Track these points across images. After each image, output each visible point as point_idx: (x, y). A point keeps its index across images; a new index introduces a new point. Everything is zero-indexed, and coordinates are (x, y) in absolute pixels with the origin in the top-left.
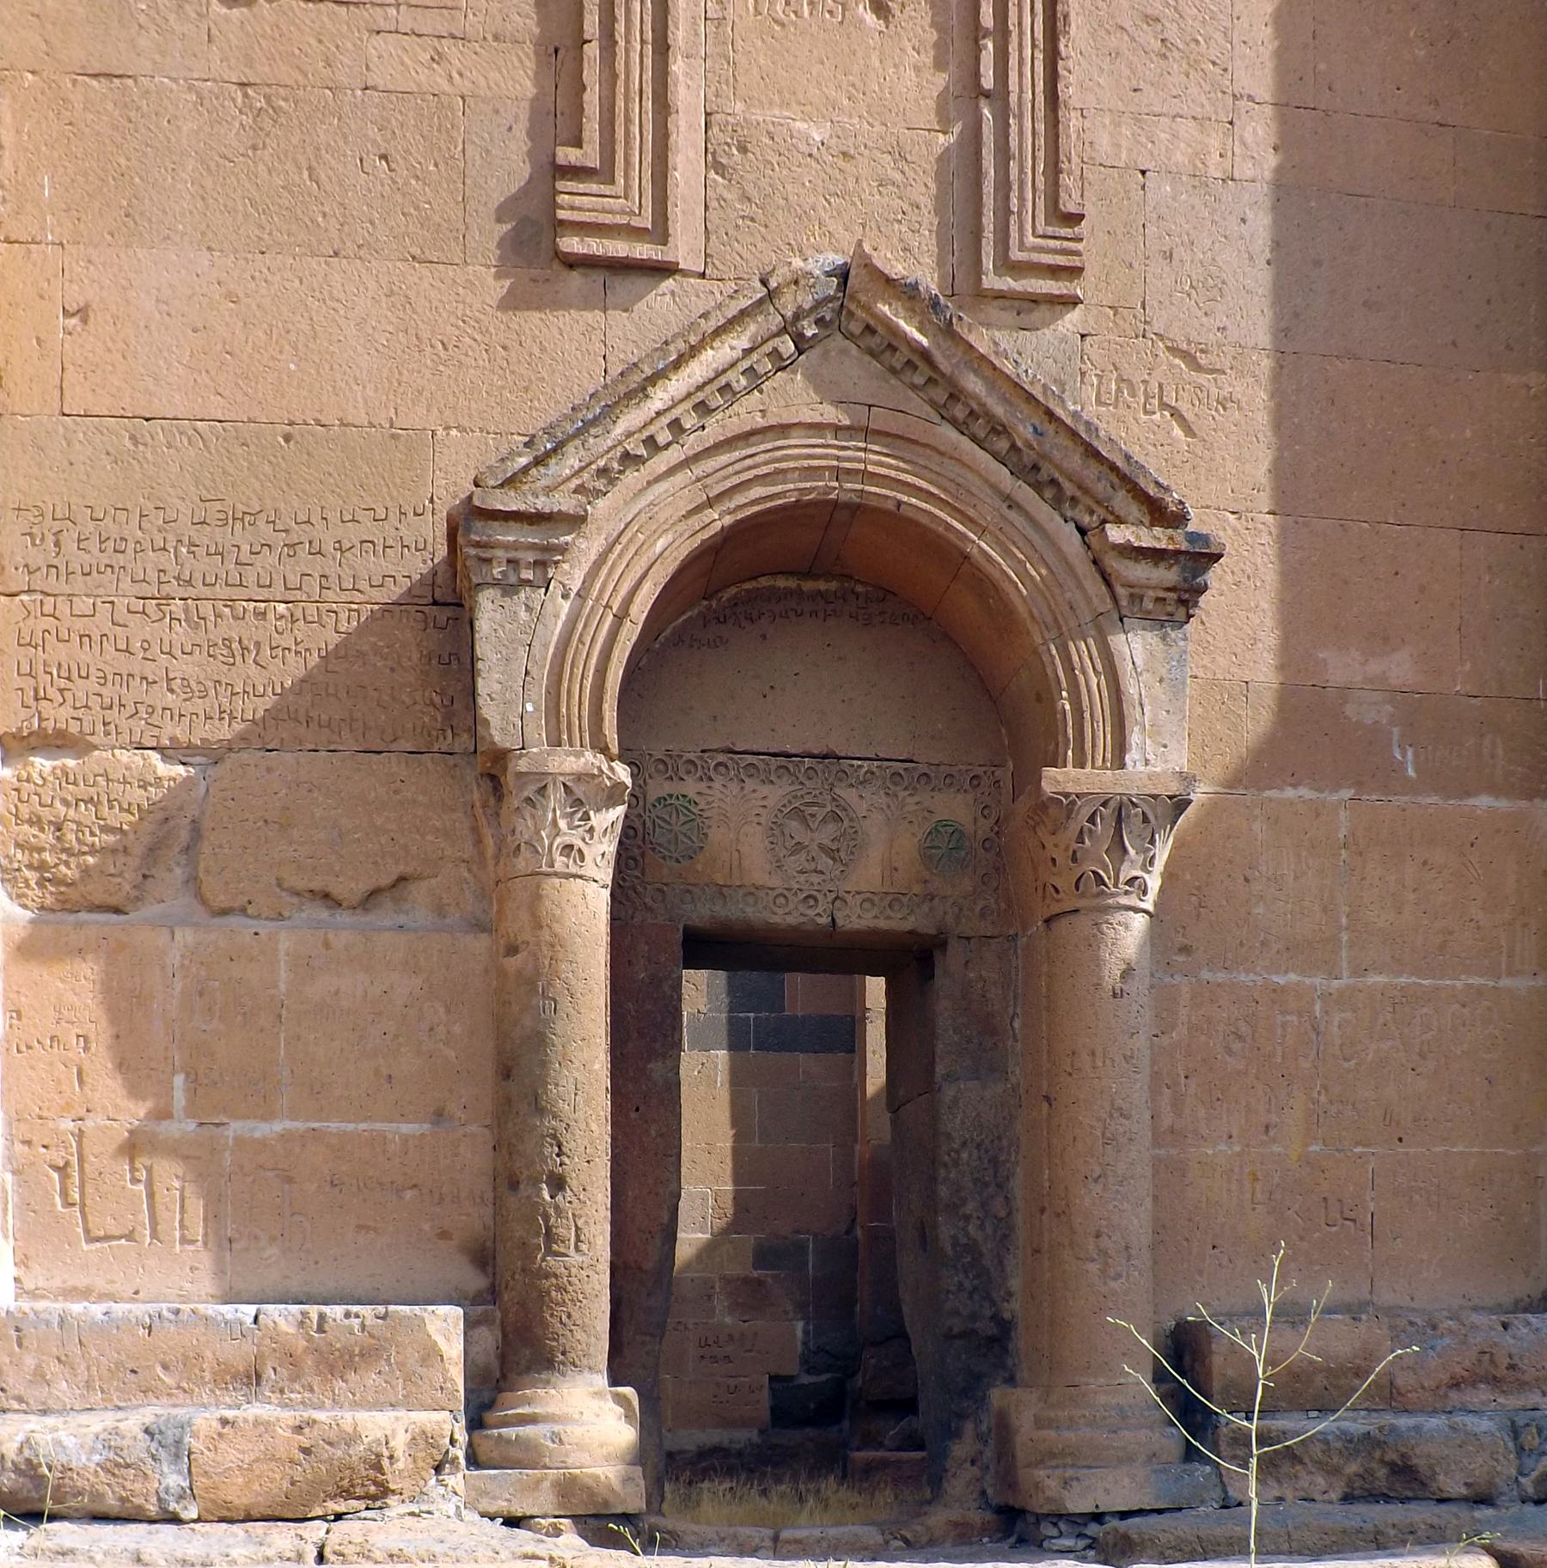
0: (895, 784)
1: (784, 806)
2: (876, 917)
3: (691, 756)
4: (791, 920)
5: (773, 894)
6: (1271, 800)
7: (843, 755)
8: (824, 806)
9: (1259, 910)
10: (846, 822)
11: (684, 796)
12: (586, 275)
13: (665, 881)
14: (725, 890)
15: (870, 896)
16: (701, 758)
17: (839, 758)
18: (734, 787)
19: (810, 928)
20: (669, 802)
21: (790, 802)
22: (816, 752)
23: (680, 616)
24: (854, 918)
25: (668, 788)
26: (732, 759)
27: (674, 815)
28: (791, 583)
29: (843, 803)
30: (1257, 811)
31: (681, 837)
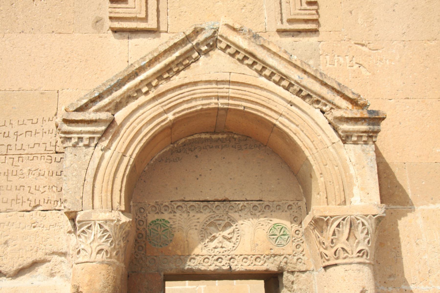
0: (256, 210)
1: (207, 221)
2: (249, 265)
3: (167, 204)
4: (212, 268)
6: (423, 210)
7: (231, 199)
8: (224, 220)
9: (426, 257)
11: (164, 220)
12: (121, 35)
13: (155, 254)
14: (182, 257)
15: (246, 256)
16: (171, 204)
17: (230, 201)
18: (185, 215)
19: (221, 271)
20: (157, 222)
21: (209, 220)
22: (220, 199)
23: (161, 151)
26: (184, 204)
27: (159, 228)
28: (208, 136)
31: (162, 236)
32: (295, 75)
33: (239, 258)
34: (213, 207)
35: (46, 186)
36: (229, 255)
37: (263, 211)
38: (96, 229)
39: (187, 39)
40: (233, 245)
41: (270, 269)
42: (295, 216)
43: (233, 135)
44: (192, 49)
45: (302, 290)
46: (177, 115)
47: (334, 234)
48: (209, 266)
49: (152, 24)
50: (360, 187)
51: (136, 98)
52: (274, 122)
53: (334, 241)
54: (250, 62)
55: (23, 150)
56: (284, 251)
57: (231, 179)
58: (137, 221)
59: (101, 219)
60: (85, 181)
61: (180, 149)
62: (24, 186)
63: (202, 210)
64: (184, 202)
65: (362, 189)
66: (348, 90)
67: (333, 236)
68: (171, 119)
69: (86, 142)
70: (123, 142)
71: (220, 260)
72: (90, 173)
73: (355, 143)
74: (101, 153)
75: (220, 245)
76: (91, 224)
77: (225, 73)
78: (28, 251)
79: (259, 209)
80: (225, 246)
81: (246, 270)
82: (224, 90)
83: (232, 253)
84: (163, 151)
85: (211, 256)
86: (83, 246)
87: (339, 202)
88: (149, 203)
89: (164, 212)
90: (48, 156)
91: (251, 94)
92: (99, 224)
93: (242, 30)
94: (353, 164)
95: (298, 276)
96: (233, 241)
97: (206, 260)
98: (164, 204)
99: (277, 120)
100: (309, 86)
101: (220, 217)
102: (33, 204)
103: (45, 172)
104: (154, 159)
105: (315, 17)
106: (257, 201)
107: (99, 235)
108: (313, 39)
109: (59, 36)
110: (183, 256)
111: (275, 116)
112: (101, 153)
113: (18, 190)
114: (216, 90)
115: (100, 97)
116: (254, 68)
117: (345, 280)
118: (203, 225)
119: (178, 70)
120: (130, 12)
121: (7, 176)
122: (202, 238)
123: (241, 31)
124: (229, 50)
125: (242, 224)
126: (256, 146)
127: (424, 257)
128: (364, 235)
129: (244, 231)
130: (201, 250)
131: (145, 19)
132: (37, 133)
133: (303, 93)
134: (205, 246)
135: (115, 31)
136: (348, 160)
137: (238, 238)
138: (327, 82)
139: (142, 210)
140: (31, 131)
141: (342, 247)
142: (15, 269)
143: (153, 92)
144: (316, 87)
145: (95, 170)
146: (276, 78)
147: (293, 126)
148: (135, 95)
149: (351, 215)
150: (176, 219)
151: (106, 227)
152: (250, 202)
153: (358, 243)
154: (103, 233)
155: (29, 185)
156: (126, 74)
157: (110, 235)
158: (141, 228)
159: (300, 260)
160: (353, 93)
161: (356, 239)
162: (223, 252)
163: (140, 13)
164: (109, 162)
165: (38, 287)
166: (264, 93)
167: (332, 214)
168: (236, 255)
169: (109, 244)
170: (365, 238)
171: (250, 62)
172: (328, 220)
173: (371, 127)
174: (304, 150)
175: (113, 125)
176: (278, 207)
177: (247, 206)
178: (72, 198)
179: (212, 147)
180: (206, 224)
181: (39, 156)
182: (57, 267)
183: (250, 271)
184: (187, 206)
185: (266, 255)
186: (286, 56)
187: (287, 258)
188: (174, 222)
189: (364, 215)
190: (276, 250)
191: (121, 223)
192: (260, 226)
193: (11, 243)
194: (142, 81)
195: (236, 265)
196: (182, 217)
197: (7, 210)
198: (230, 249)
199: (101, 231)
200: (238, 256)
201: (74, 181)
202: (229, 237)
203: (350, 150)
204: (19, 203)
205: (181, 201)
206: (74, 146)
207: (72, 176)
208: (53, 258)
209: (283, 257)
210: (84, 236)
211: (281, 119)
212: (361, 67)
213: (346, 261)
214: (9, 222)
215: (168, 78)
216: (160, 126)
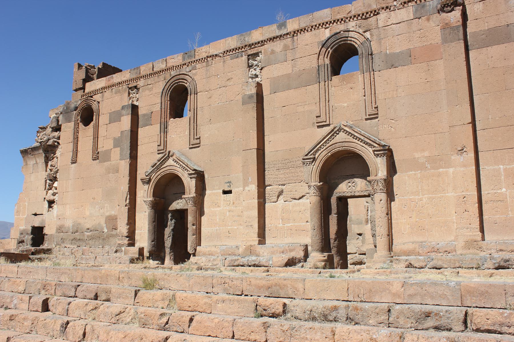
4: (349, 195)
9: (407, 189)
28: (348, 155)
32: (362, 138)
47: (373, 185)
49: (328, 123)
51: (320, 150)
69: (309, 164)
73: (380, 157)
100: (366, 141)
105: (376, 113)
108: (377, 120)
111: (358, 151)
115: (311, 151)
124: (344, 132)
128: (381, 184)
131: (326, 122)
133: (365, 143)
135: (319, 127)
144: (369, 141)
151: (315, 187)
186: (359, 132)
190: (368, 189)
213: (377, 192)
215: (328, 143)
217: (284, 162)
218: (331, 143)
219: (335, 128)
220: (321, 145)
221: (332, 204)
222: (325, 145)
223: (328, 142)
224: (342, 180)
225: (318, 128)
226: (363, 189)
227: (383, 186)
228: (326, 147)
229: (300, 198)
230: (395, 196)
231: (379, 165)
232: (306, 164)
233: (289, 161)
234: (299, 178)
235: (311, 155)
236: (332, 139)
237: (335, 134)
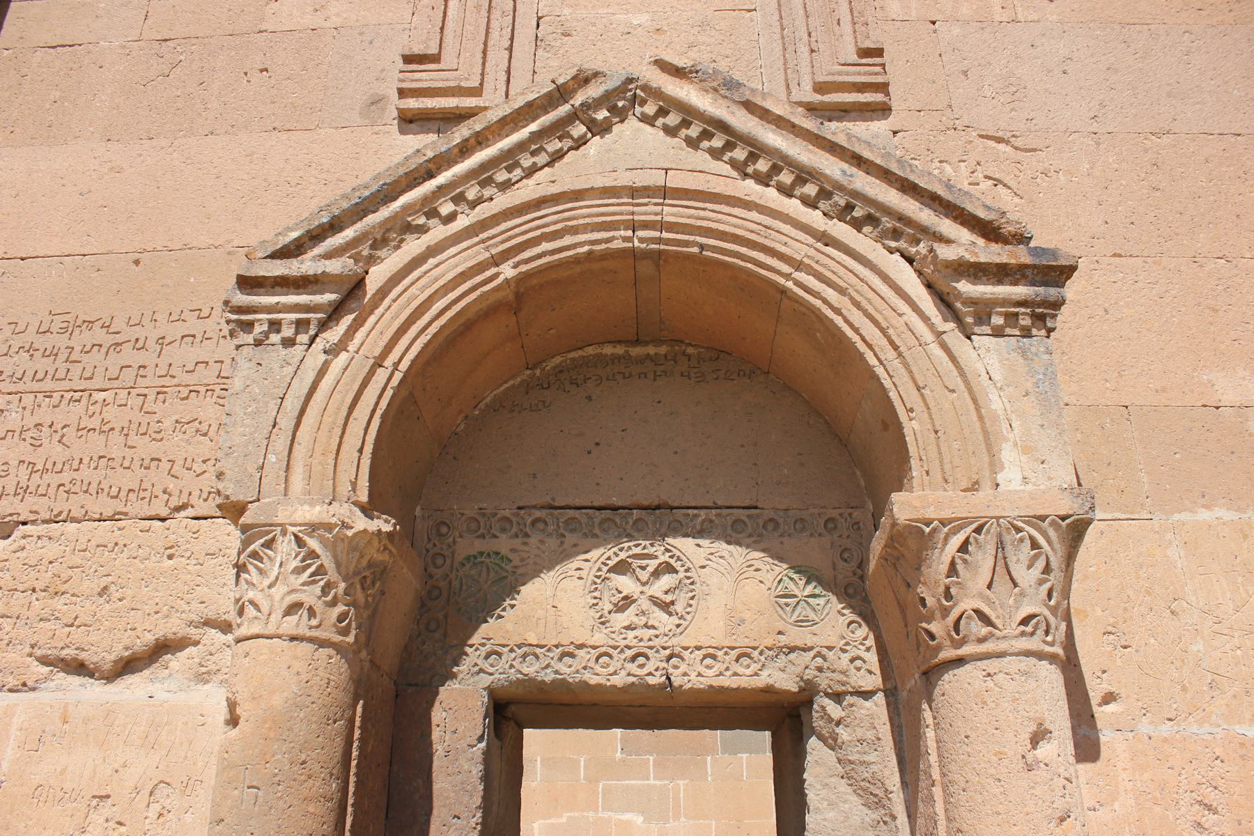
1: (609, 558)
2: (721, 674)
3: (507, 513)
4: (619, 680)
5: (595, 653)
7: (676, 504)
8: (656, 557)
9: (1198, 647)
10: (682, 575)
11: (497, 554)
15: (711, 651)
17: (672, 508)
22: (646, 503)
24: (693, 676)
25: (479, 545)
26: (551, 514)
27: (484, 573)
28: (620, 350)
29: (678, 553)
30: (1169, 536)
33: (693, 656)
34: (627, 523)
35: (209, 459)
36: (664, 648)
37: (760, 535)
38: (286, 546)
39: (561, 94)
40: (678, 622)
41: (777, 685)
42: (843, 548)
43: (683, 348)
44: (572, 117)
45: (865, 744)
46: (524, 268)
47: (952, 570)
48: (611, 675)
50: (1019, 443)
51: (422, 230)
52: (782, 281)
53: (953, 591)
54: (717, 142)
55: (171, 376)
56: (815, 638)
57: (676, 453)
58: (430, 554)
59: (300, 521)
60: (274, 426)
61: (549, 383)
62: (160, 460)
63: (597, 531)
64: (552, 511)
65: (1026, 450)
66: (974, 200)
67: (948, 577)
68: (509, 277)
69: (288, 332)
70: (381, 333)
71: (641, 660)
72: (289, 408)
73: (998, 333)
74: (323, 357)
75: (644, 619)
76: (274, 533)
77: (654, 171)
78: (149, 615)
79: (750, 530)
80: (656, 624)
81: (711, 687)
82: (648, 210)
83: (675, 641)
84: (506, 386)
85: (619, 650)
86: (251, 594)
87: (964, 484)
88: (461, 511)
89: (498, 534)
90: (222, 389)
91: (720, 216)
92: (296, 536)
93: (697, 72)
94: (999, 385)
95: (852, 705)
96: (678, 611)
97: (605, 659)
98: (501, 513)
99: (788, 276)
101: (644, 548)
102: (174, 502)
103: (210, 425)
104: (482, 405)
105: (880, 79)
106: (744, 508)
107: (295, 563)
109: (284, 136)
110: (542, 647)
111: (785, 268)
112: (323, 357)
113: (145, 468)
114: (631, 208)
115: (334, 226)
116: (726, 158)
117: (985, 703)
118: (599, 570)
119: (535, 164)
120: (445, 78)
121: (127, 435)
122: (595, 601)
123: (694, 75)
125: (703, 567)
126: (742, 373)
127: (1194, 648)
129: (708, 585)
130: (590, 632)
132: (206, 339)
133: (858, 213)
134: (603, 623)
136: (983, 373)
137: (691, 602)
138: (916, 182)
139: (444, 530)
140: (194, 336)
141: (975, 606)
142: (113, 657)
143: (468, 215)
145: (303, 399)
146: (786, 178)
147: (830, 294)
148: (422, 220)
149: (998, 518)
150: (528, 552)
151: (313, 544)
152: (725, 511)
153: (1022, 594)
154: (303, 561)
155: (171, 458)
156: (402, 171)
157: (322, 565)
158: (438, 573)
159: (858, 663)
160: (988, 208)
161: (1015, 585)
162: (650, 640)
163: (467, 79)
164: (339, 381)
165: (161, 705)
166: (754, 215)
167: (946, 514)
168: (686, 649)
169: (318, 591)
170: (1041, 582)
171: (717, 142)
172: (934, 530)
173: (1041, 290)
174: (862, 351)
175: (360, 293)
176: (798, 526)
177: (717, 522)
178: (237, 469)
179: (630, 375)
180: (608, 565)
181: (202, 389)
182: (213, 658)
183: (722, 690)
184: (558, 519)
185: (766, 648)
187: (824, 658)
188: (522, 560)
189: (1034, 517)
190: (796, 636)
191: (350, 533)
192: (751, 573)
193: (115, 593)
194: (440, 188)
195: (685, 674)
196: (543, 547)
197: (114, 515)
198: (670, 631)
199: (300, 552)
200: (690, 650)
201: (248, 426)
202: (667, 601)
203: (988, 350)
204: (143, 499)
205: (543, 507)
206: (258, 343)
207: (245, 414)
208: (205, 636)
209: (812, 653)
210: (256, 567)
211: (801, 276)
212: (1000, 186)
214: (116, 544)
215: (506, 186)
216: (478, 293)
217: (62, 341)
218: (528, 190)
219: (587, 81)
220: (441, 190)
221: (439, 749)
222: (471, 194)
223: (501, 176)
224: (552, 543)
225: (402, 132)
226: (759, 630)
227: (1050, 596)
228: (483, 211)
229: (128, 666)
230: (1096, 709)
231: (993, 395)
232: (258, 329)
233: (108, 340)
234: (158, 478)
235: (328, 256)
236: (542, 159)
237: (579, 130)
